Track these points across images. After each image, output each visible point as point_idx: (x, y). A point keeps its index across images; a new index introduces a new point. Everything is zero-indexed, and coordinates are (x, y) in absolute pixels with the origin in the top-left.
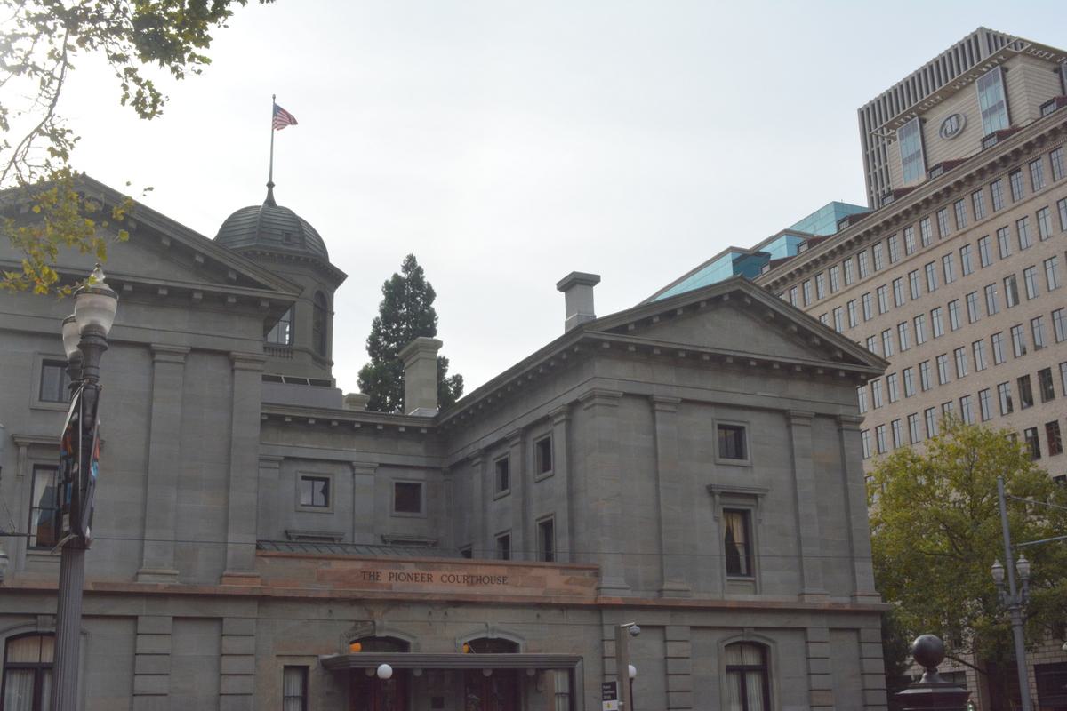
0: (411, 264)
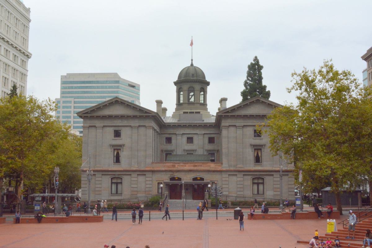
0: (256, 59)
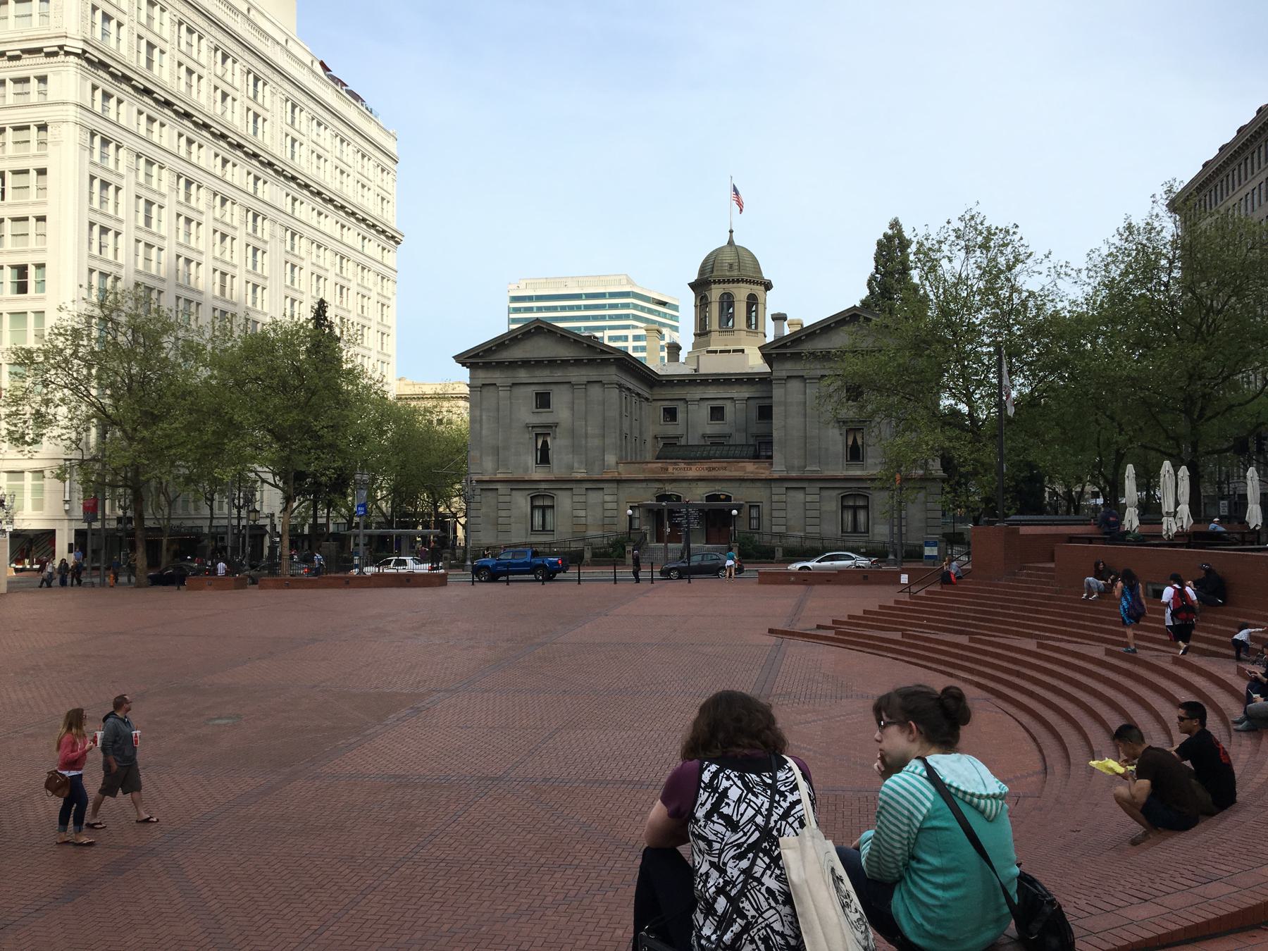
0: (895, 224)
